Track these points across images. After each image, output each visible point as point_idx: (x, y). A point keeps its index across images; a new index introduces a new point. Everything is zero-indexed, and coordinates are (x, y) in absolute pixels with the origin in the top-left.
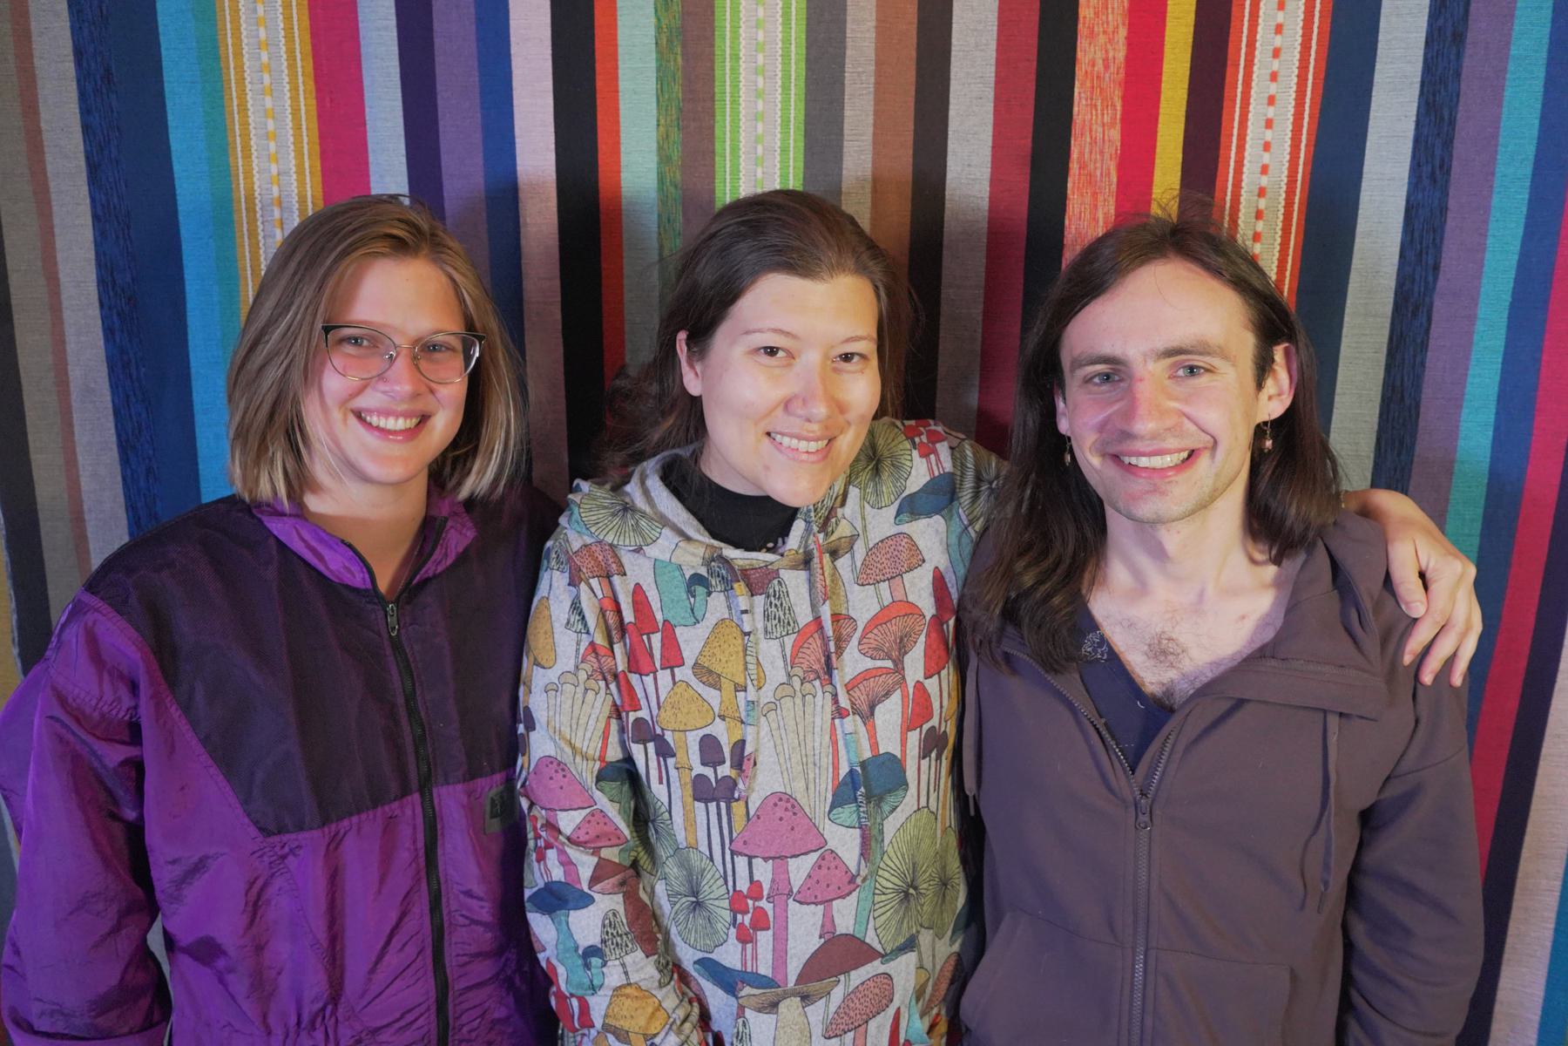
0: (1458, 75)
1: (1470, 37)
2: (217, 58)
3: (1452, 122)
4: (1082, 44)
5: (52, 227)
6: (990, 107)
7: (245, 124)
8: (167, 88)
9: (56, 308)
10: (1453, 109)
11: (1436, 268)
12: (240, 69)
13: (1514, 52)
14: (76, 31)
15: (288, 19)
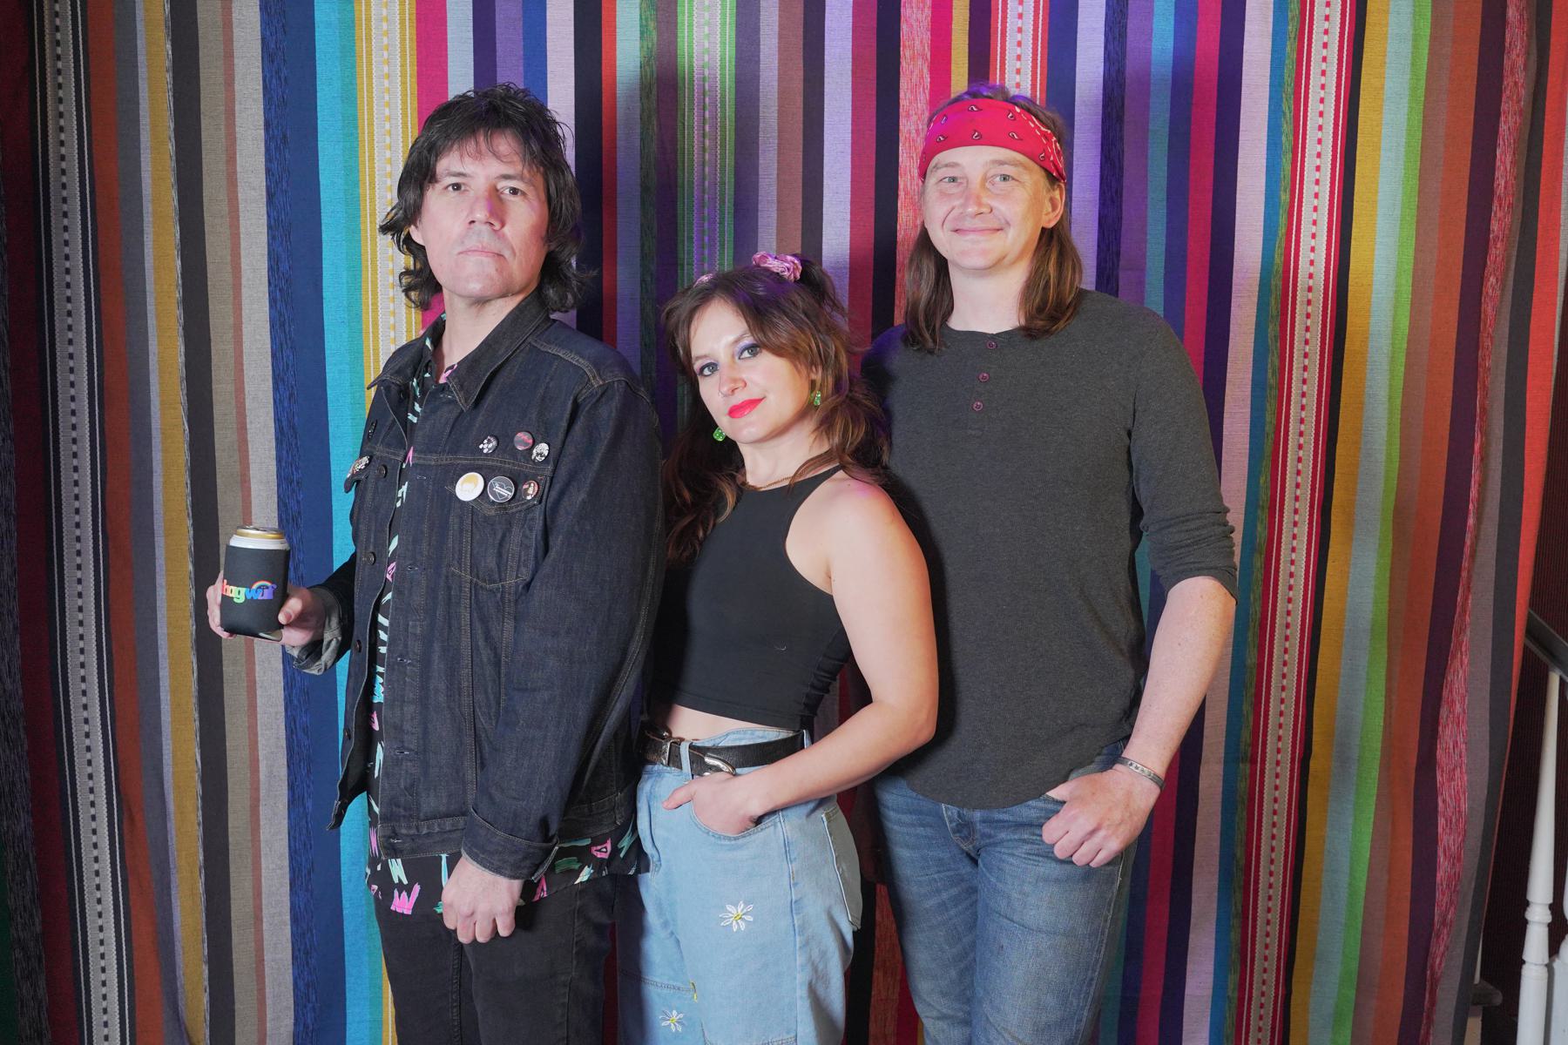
0: (1122, 139)
1: (1126, 118)
2: (356, 128)
3: (1121, 168)
4: (902, 121)
5: (238, 234)
6: (849, 157)
7: (372, 168)
8: (320, 144)
9: (237, 287)
10: (1121, 160)
11: (1118, 254)
12: (371, 134)
13: (1151, 127)
14: (267, 111)
15: (404, 103)
